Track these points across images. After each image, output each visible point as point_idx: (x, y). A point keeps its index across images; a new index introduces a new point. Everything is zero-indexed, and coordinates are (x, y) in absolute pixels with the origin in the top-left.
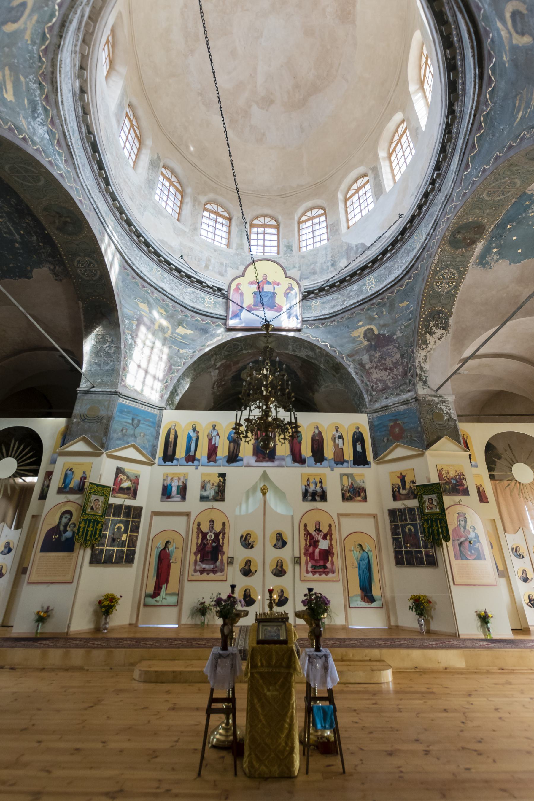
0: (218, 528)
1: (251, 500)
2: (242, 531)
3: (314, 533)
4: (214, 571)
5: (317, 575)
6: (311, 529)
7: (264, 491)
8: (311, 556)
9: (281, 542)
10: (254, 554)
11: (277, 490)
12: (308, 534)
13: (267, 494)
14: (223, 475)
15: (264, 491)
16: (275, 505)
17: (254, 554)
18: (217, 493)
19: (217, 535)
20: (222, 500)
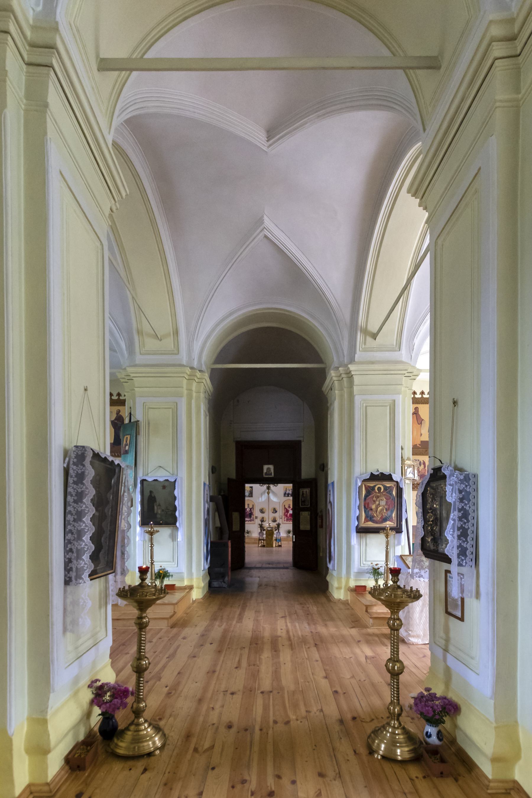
0: (251, 506)
1: (263, 496)
2: (260, 507)
3: (288, 508)
4: (250, 521)
5: (288, 522)
6: (287, 507)
7: (268, 493)
8: (286, 516)
9: (275, 511)
10: (265, 515)
11: (273, 492)
12: (285, 508)
13: (270, 494)
14: (251, 487)
15: (268, 493)
16: (273, 498)
17: (265, 515)
18: (249, 494)
19: (251, 509)
20: (252, 496)
